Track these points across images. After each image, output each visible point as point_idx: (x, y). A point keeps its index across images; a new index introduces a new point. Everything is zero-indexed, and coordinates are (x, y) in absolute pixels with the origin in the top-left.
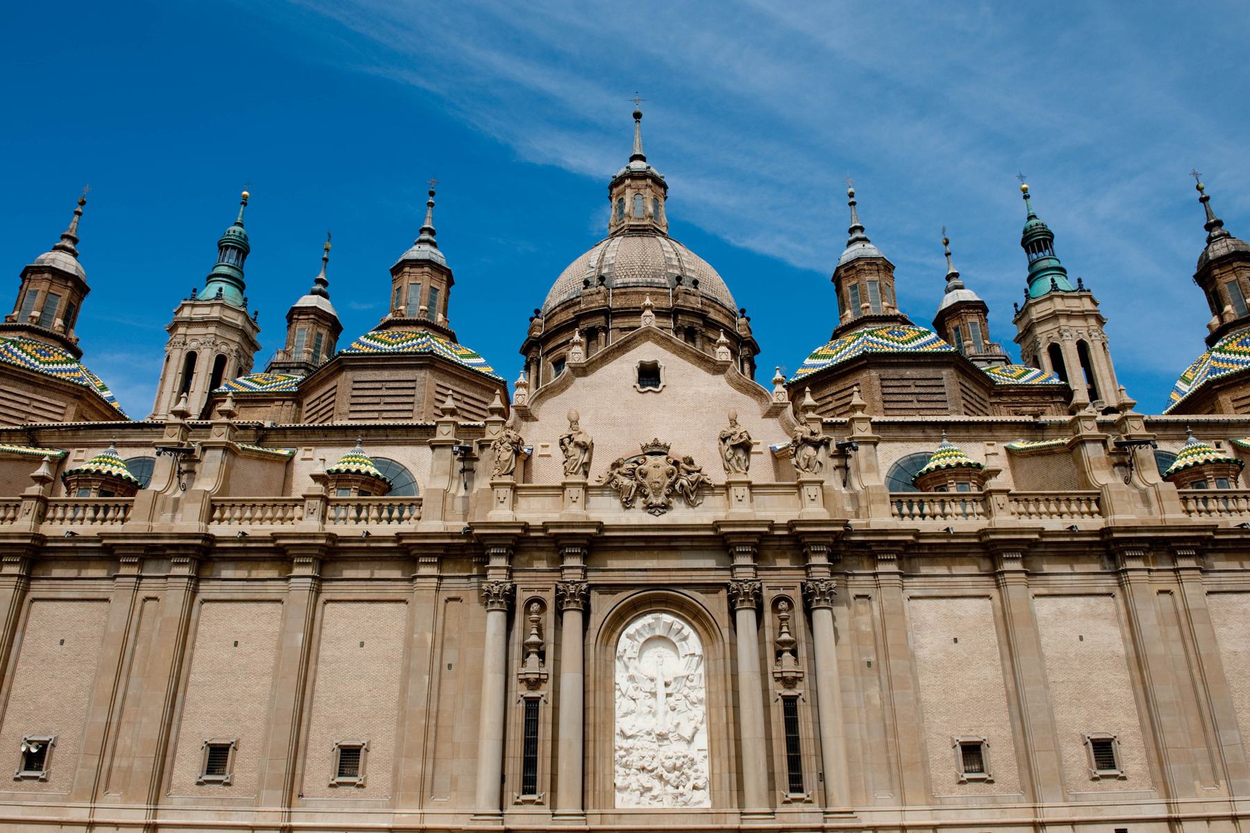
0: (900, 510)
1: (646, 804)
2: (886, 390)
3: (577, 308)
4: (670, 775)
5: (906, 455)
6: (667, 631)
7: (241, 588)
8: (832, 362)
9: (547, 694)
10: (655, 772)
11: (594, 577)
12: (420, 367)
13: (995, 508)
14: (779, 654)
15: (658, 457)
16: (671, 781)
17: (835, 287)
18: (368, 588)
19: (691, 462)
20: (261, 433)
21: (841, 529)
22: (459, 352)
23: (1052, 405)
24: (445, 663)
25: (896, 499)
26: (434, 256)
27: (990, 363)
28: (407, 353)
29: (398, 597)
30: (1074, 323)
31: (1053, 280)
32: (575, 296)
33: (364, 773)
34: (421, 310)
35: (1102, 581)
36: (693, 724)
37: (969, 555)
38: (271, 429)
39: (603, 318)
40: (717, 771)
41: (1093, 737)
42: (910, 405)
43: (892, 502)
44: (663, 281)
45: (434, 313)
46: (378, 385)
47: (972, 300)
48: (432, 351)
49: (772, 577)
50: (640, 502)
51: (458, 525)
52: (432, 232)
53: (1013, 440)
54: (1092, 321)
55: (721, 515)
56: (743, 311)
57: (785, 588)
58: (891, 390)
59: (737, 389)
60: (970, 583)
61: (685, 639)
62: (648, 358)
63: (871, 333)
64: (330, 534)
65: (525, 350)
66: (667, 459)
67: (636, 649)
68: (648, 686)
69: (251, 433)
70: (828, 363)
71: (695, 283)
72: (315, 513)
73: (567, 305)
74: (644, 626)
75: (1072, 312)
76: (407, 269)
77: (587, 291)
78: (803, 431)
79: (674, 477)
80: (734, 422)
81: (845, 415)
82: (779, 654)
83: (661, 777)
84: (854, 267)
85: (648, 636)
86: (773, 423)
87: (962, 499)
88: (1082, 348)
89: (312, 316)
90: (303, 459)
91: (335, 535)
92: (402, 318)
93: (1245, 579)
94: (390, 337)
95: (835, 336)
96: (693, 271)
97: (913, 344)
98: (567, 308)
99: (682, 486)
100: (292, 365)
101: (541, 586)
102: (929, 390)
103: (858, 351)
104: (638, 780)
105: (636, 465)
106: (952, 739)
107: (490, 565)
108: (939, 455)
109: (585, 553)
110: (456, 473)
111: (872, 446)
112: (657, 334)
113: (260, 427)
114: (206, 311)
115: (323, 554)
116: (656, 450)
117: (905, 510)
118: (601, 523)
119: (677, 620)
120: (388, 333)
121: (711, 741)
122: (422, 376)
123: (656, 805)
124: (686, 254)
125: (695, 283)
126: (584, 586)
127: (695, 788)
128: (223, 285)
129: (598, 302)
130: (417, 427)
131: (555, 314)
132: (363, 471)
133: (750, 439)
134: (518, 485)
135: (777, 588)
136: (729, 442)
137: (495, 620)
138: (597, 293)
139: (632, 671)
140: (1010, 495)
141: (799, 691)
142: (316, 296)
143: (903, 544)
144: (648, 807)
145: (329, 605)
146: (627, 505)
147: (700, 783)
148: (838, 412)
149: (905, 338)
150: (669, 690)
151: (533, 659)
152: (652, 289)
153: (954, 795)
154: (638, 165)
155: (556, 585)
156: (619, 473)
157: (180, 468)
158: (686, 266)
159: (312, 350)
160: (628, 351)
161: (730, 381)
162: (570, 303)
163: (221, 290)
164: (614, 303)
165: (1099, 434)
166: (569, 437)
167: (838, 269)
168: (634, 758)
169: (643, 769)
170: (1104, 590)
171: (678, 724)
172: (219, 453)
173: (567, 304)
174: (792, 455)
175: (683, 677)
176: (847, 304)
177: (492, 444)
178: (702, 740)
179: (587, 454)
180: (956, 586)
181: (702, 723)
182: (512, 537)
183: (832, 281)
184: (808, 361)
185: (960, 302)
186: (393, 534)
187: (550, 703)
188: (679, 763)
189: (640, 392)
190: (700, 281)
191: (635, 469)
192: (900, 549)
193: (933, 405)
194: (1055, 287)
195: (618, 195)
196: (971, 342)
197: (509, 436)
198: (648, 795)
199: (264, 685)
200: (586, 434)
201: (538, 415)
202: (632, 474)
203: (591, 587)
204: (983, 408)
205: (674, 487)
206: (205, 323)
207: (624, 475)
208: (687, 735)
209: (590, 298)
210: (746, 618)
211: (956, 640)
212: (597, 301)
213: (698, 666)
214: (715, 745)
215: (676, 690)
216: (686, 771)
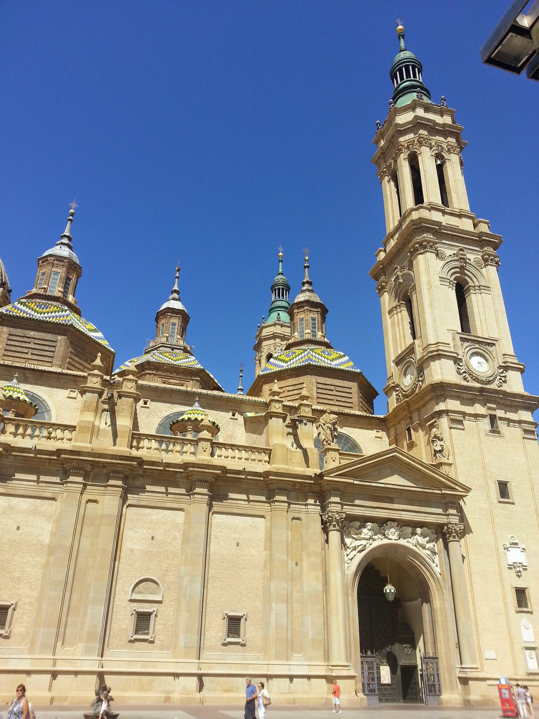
23: (191, 381)
27: (173, 350)
31: (279, 314)
35: (50, 489)
42: (23, 356)
58: (13, 343)
75: (285, 335)
84: (47, 260)
93: (159, 498)
170: (50, 495)
193: (41, 358)
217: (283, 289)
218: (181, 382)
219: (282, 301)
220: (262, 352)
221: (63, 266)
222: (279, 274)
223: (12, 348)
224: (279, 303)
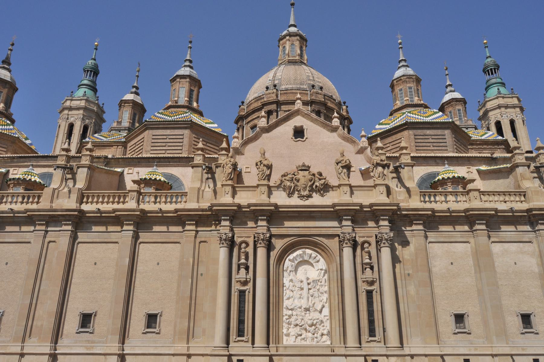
0: (425, 199)
1: (299, 342)
2: (417, 141)
3: (262, 101)
4: (310, 328)
5: (426, 173)
6: (309, 258)
7: (98, 236)
8: (390, 126)
9: (250, 289)
10: (303, 326)
12: (185, 128)
13: (472, 198)
14: (364, 270)
15: (305, 172)
16: (311, 331)
17: (391, 90)
18: (161, 236)
19: (320, 174)
20: (106, 160)
21: (396, 208)
22: (205, 121)
23: (499, 150)
24: (199, 273)
25: (422, 194)
26: (192, 73)
28: (179, 121)
29: (175, 241)
30: (509, 110)
31: (498, 89)
32: (261, 94)
33: (159, 327)
34: (186, 100)
35: (526, 235)
36: (321, 304)
37: (459, 221)
38: (112, 159)
39: (275, 105)
41: (522, 313)
42: (428, 148)
43: (420, 195)
44: (305, 87)
45: (192, 102)
46: (165, 137)
47: (459, 97)
48: (191, 120)
49: (361, 231)
50: (296, 195)
51: (205, 205)
52: (190, 61)
53: (481, 165)
54: (518, 109)
55: (336, 201)
56: (344, 103)
57: (368, 237)
58: (419, 141)
59: (343, 140)
60: (460, 236)
61: (318, 261)
62: (298, 124)
63: (409, 112)
64: (142, 209)
65: (237, 122)
66: (309, 173)
68: (298, 285)
69: (101, 160)
70: (388, 127)
71: (321, 88)
72: (134, 199)
75: (507, 105)
76: (178, 80)
77: (267, 92)
78: (377, 159)
81: (396, 153)
82: (364, 270)
83: (306, 330)
84: (401, 80)
87: (455, 194)
88: (512, 122)
89: (131, 104)
90: (127, 174)
91: (144, 210)
92: (176, 104)
94: (170, 113)
95: (391, 114)
96: (320, 82)
97: (431, 118)
98: (257, 100)
99: (316, 186)
100: (121, 129)
101: (247, 235)
102: (438, 141)
103: (403, 121)
104: (293, 331)
105: (294, 176)
106: (450, 312)
107: (221, 225)
108: (443, 173)
109: (268, 220)
110: (204, 180)
111: (411, 167)
112: (303, 112)
113: (106, 157)
114: (78, 102)
115: (138, 219)
116: (303, 168)
117: (427, 199)
118: (276, 204)
119: (313, 252)
120: (169, 111)
121: (330, 312)
122: (187, 132)
123: (303, 343)
124: (317, 74)
125: (321, 88)
126: (268, 235)
128: (86, 90)
129: (273, 98)
130: (184, 158)
131: (252, 103)
132: (158, 179)
133: (350, 163)
134: (235, 185)
135: (363, 237)
136: (340, 165)
137: (223, 252)
138: (273, 93)
140: (480, 192)
141: (375, 288)
142: (133, 95)
143: (426, 216)
144: (299, 343)
145: (142, 244)
146: (290, 195)
148: (392, 151)
149: (426, 115)
150: (310, 286)
151: (243, 271)
153: (451, 340)
154: (293, 29)
155: (254, 235)
156: (285, 179)
157: (66, 177)
159: (132, 121)
160: (289, 120)
161: (339, 136)
162: (259, 98)
163: (85, 92)
164: (281, 98)
165: (526, 162)
166: (261, 161)
167: (393, 80)
170: (527, 240)
171: (314, 303)
172: (86, 170)
173: (258, 98)
174: (371, 171)
175: (317, 280)
176: (397, 98)
177: (222, 165)
178: (326, 311)
179: (269, 170)
180: (452, 237)
181: (326, 303)
182: (232, 211)
183: (390, 87)
184: (377, 127)
185: (453, 99)
186: (173, 210)
188: (315, 322)
189: (295, 141)
190: (323, 87)
191: (293, 178)
192: (425, 218)
193: (440, 148)
194: (499, 93)
196: (458, 119)
197: (230, 161)
198: (299, 338)
199: (109, 284)
200: (269, 160)
201: (244, 152)
202: (292, 180)
204: (465, 150)
205: (312, 187)
206: (78, 109)
207: (288, 180)
208: (319, 308)
209: (269, 96)
210: (347, 251)
211: (452, 263)
212: (273, 97)
213: (324, 275)
214: (333, 313)
215: (314, 287)
216: (318, 326)
217: (495, 69)
218: (492, 151)
219: (496, 78)
220: (490, 121)
221: (413, 81)
222: (487, 58)
223: (421, 144)
224: (493, 81)
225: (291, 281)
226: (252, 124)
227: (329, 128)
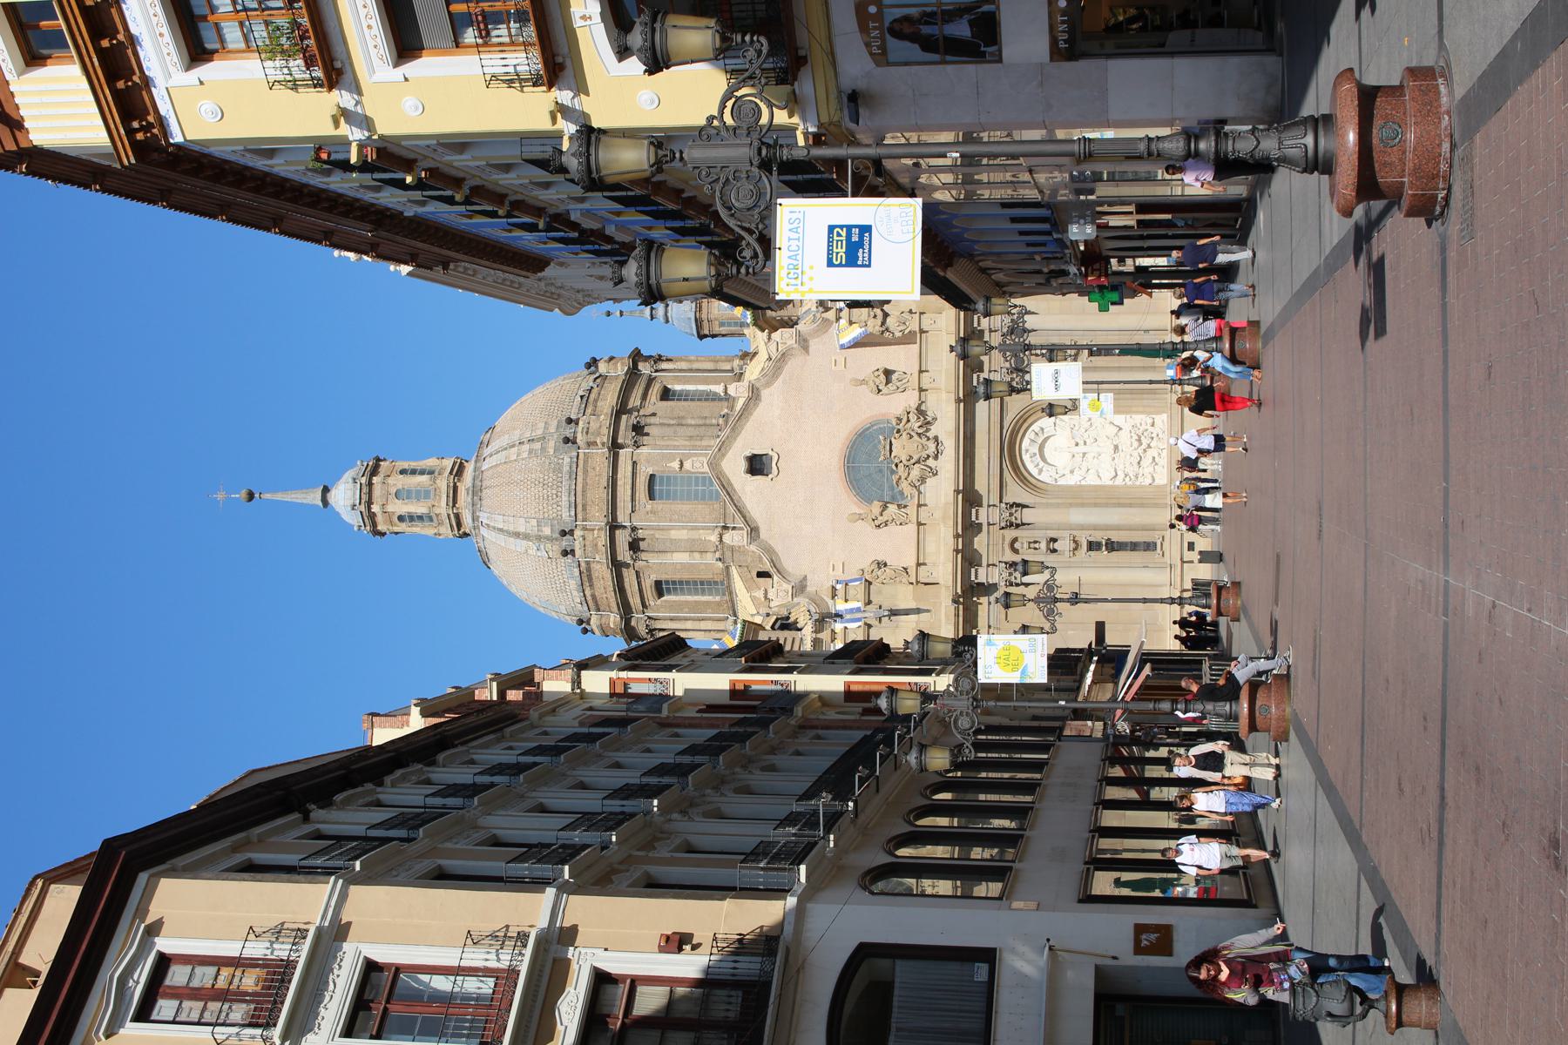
11: (995, 499)
32: (577, 570)
40: (1141, 409)
44: (567, 460)
50: (931, 462)
59: (777, 377)
61: (1042, 429)
62: (743, 465)
67: (1050, 468)
68: (1078, 458)
73: (586, 577)
74: (1032, 462)
77: (578, 552)
79: (912, 433)
80: (863, 382)
85: (1039, 459)
86: (814, 344)
123: (1165, 453)
125: (569, 421)
127: (1153, 425)
131: (594, 597)
139: (1067, 472)
147: (1150, 421)
150: (1081, 443)
152: (580, 473)
158: (540, 432)
162: (584, 575)
164: (598, 519)
168: (1131, 471)
169: (1139, 463)
173: (585, 579)
187: (1090, 532)
195: (391, 523)
203: (1001, 502)
209: (589, 549)
225: (1072, 472)
226: (649, 593)
227: (752, 405)
